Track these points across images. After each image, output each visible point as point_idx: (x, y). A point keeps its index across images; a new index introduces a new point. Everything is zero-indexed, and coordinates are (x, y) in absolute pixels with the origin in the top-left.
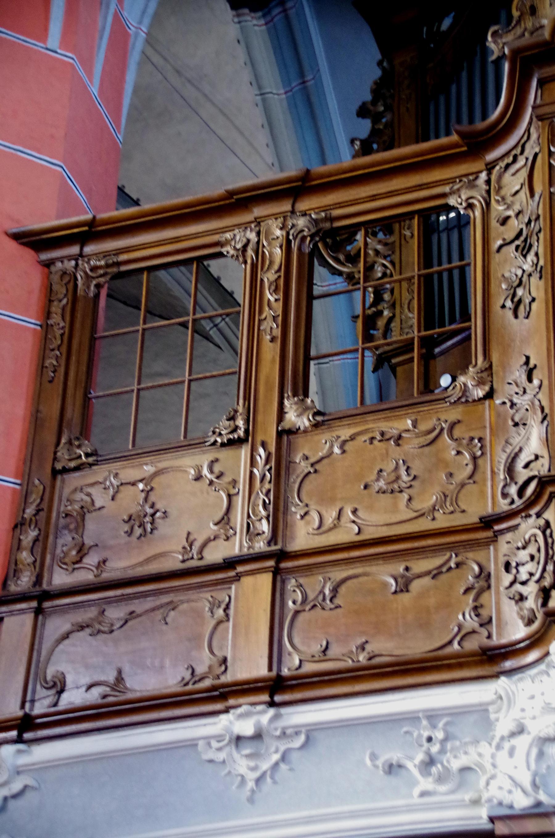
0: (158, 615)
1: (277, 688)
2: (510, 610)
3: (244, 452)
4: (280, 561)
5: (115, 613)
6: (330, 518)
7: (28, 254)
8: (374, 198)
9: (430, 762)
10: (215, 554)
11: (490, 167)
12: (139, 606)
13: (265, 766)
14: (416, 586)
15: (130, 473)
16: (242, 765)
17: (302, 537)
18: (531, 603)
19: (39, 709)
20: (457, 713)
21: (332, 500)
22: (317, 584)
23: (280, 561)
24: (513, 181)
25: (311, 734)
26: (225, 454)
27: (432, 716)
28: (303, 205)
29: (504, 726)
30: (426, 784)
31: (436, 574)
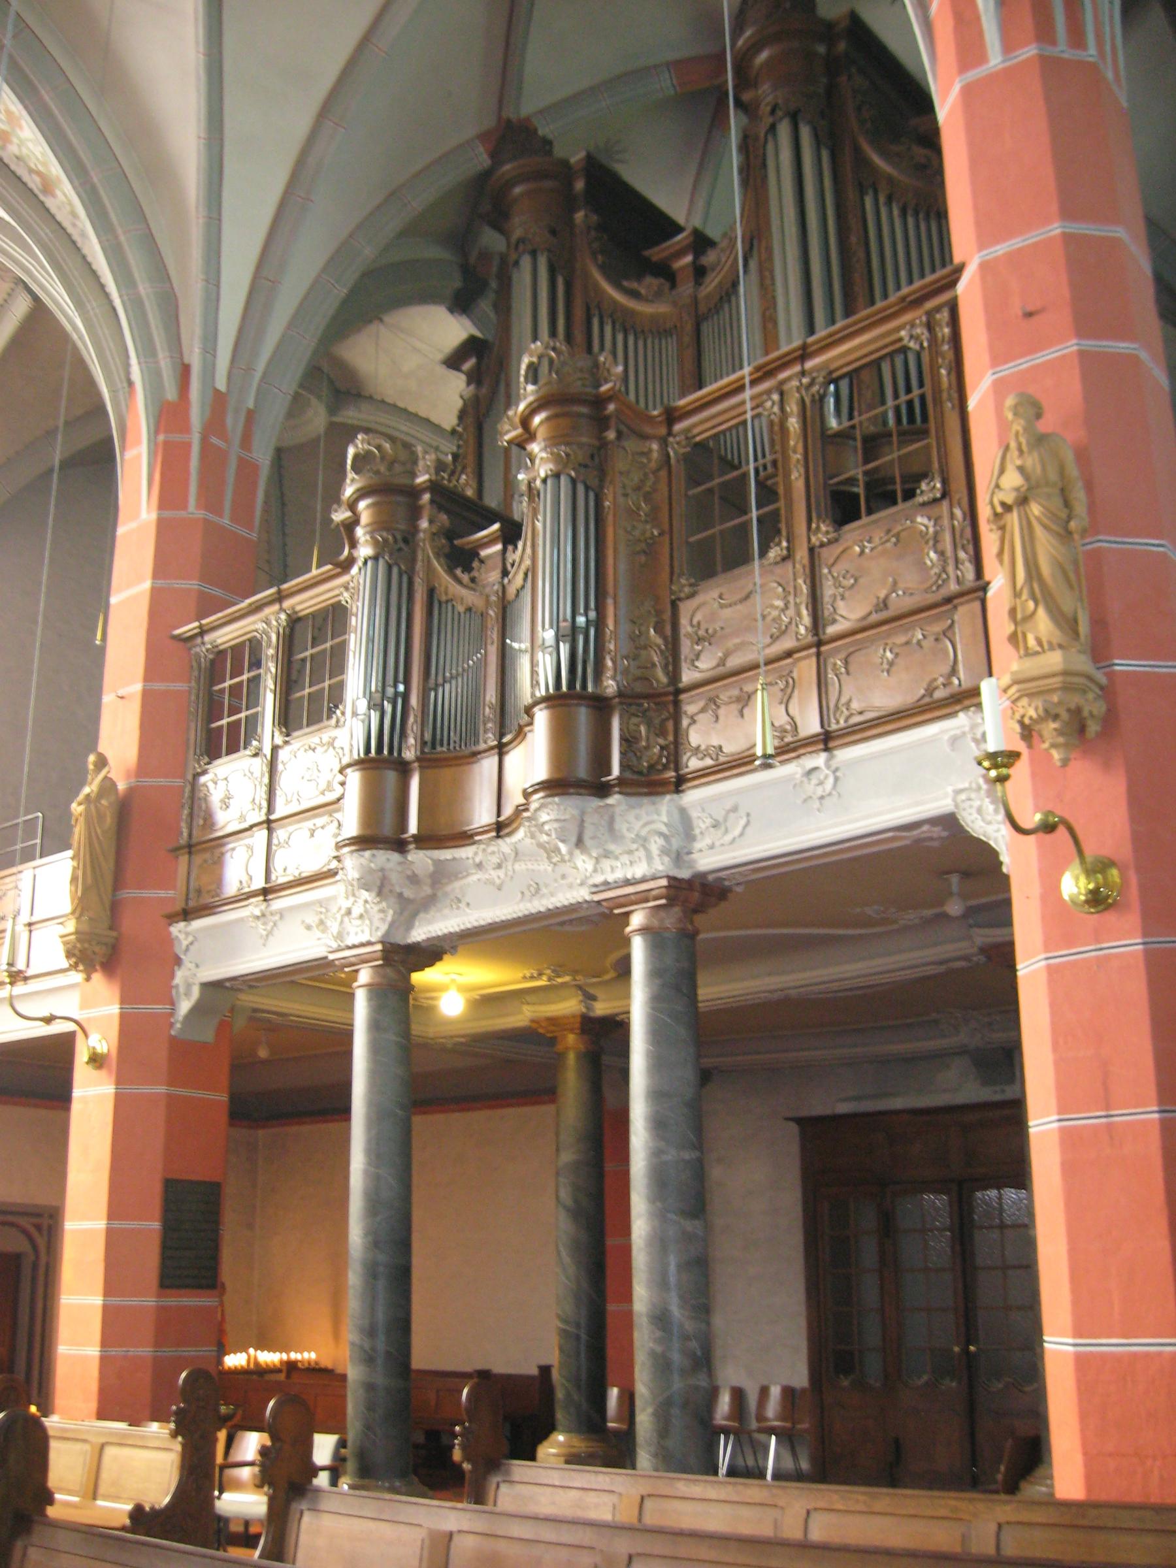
7: (181, 644)
8: (312, 598)
13: (269, 928)
19: (192, 904)
27: (320, 903)
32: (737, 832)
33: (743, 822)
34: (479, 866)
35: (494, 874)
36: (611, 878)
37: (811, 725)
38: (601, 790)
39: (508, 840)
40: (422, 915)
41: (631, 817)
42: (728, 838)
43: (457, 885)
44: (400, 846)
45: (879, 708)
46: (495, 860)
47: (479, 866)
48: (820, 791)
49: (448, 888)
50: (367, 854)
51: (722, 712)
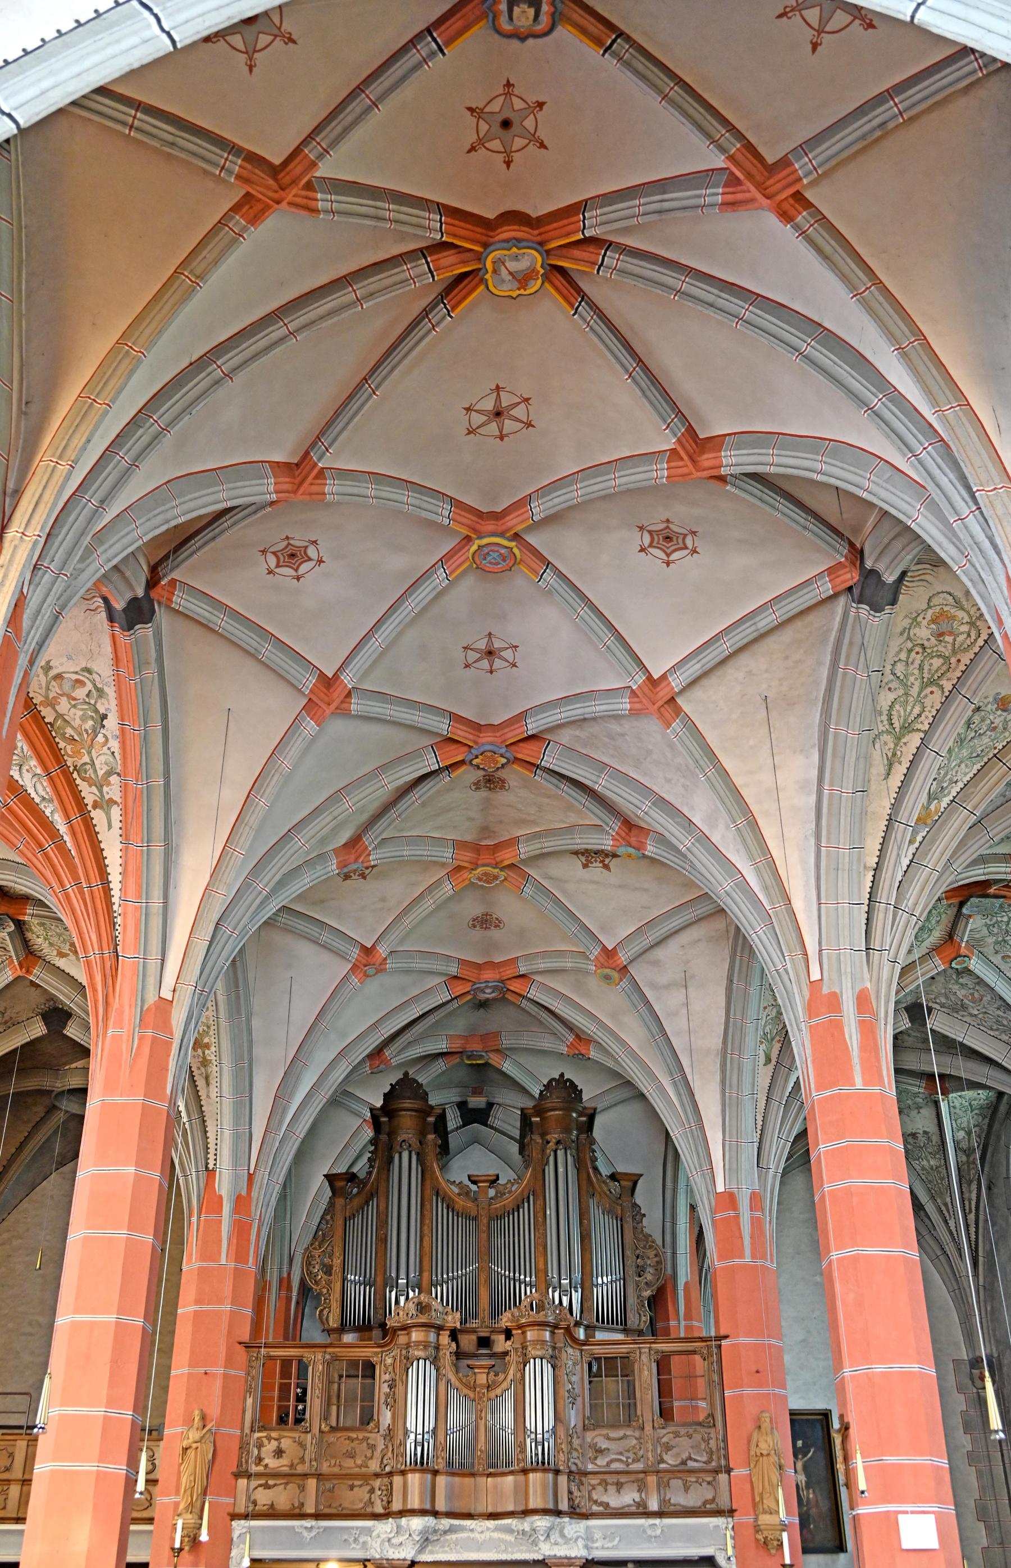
0: (283, 1486)
1: (317, 1516)
2: (378, 1502)
3: (309, 1436)
4: (319, 1476)
5: (271, 1482)
6: (333, 1462)
9: (356, 1540)
10: (300, 1469)
11: (382, 1352)
12: (278, 1482)
14: (356, 1489)
15: (274, 1434)
16: (305, 1534)
17: (325, 1468)
18: (384, 1503)
20: (363, 1528)
21: (333, 1457)
22: (329, 1485)
23: (319, 1476)
24: (389, 1361)
25: (326, 1529)
26: (303, 1435)
27: (357, 1528)
28: (329, 1350)
29: (374, 1534)
30: (353, 1545)
31: (360, 1486)
32: (615, 1542)
33: (617, 1539)
34: (472, 1530)
35: (478, 1536)
36: (558, 1554)
37: (654, 1506)
38: (558, 1513)
39: (492, 1522)
40: (430, 1548)
41: (569, 1528)
42: (610, 1545)
43: (454, 1536)
44: (435, 1514)
45: (683, 1506)
46: (480, 1529)
47: (472, 1530)
48: (653, 1534)
49: (448, 1537)
50: (426, 1518)
51: (609, 1487)
